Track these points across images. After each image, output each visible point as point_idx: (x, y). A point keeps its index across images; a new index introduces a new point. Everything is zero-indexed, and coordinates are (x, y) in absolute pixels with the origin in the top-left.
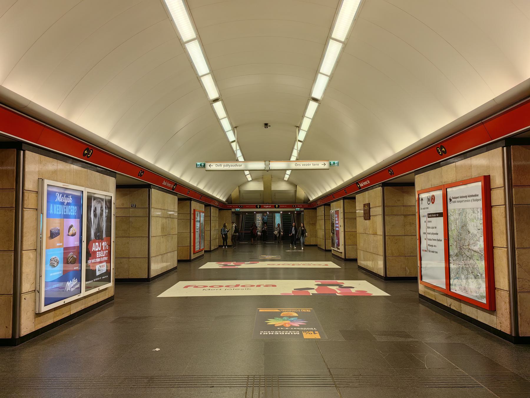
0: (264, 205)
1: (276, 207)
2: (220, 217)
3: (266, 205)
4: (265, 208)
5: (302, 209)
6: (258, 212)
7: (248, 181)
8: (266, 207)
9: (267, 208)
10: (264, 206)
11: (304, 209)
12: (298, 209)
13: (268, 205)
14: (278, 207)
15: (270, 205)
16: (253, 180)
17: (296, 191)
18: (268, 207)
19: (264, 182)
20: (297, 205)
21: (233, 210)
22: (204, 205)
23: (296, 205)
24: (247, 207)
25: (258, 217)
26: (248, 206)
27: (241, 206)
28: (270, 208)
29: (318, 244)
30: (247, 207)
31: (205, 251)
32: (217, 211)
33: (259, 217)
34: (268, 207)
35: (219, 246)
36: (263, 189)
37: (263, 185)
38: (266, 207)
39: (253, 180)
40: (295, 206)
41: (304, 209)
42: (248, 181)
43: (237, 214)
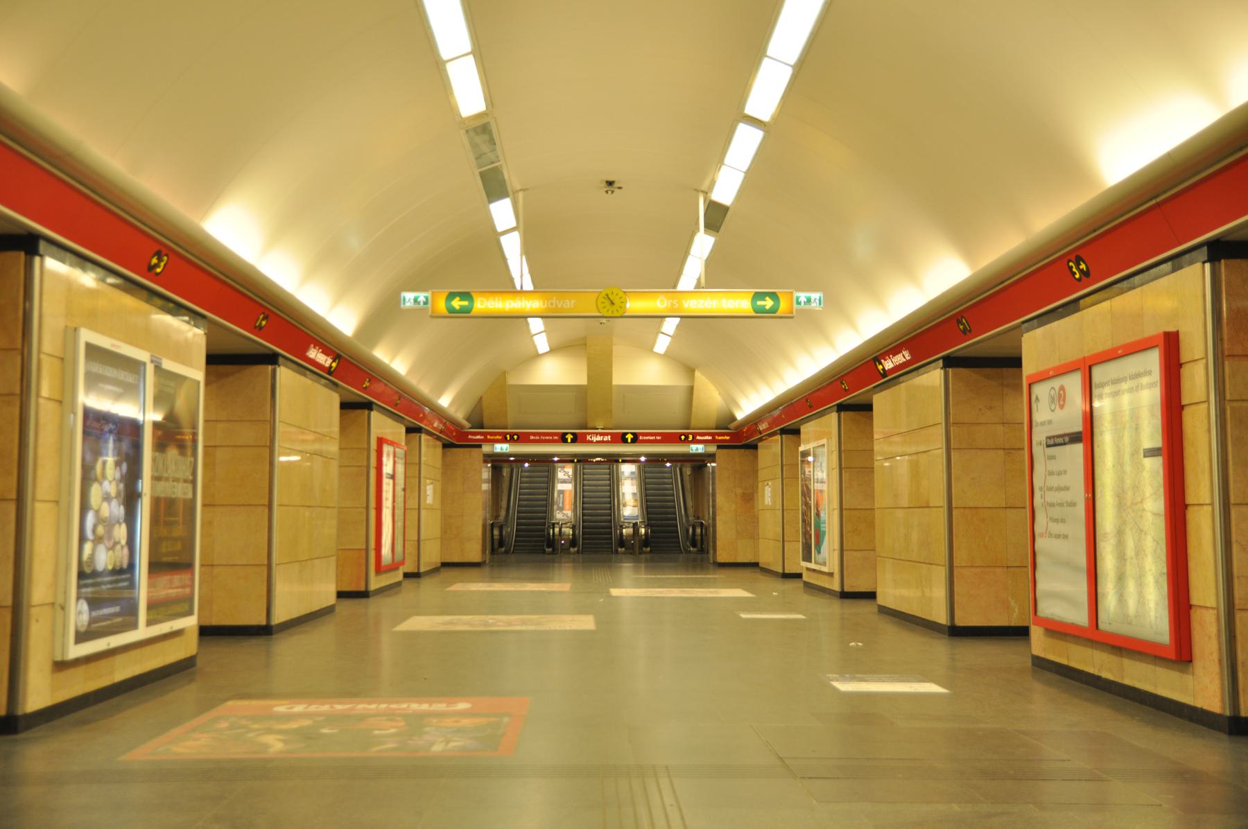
0: (589, 434)
1: (624, 441)
2: (447, 469)
3: (594, 433)
4: (592, 442)
5: (712, 449)
6: (567, 459)
7: (537, 356)
8: (595, 439)
9: (597, 442)
10: (588, 438)
11: (719, 447)
12: (697, 449)
13: (601, 434)
14: (635, 439)
15: (607, 434)
16: (554, 350)
17: (691, 390)
18: (599, 438)
19: (589, 359)
20: (694, 435)
21: (486, 448)
22: (403, 430)
23: (690, 433)
24: (532, 438)
25: (560, 475)
26: (534, 434)
27: (512, 437)
28: (607, 442)
29: (760, 562)
30: (532, 438)
31: (406, 575)
32: (439, 450)
33: (565, 481)
34: (599, 438)
35: (445, 565)
36: (582, 380)
37: (585, 368)
38: (595, 439)
39: (554, 350)
40: (687, 437)
41: (719, 447)
42: (537, 356)
43: (497, 462)
